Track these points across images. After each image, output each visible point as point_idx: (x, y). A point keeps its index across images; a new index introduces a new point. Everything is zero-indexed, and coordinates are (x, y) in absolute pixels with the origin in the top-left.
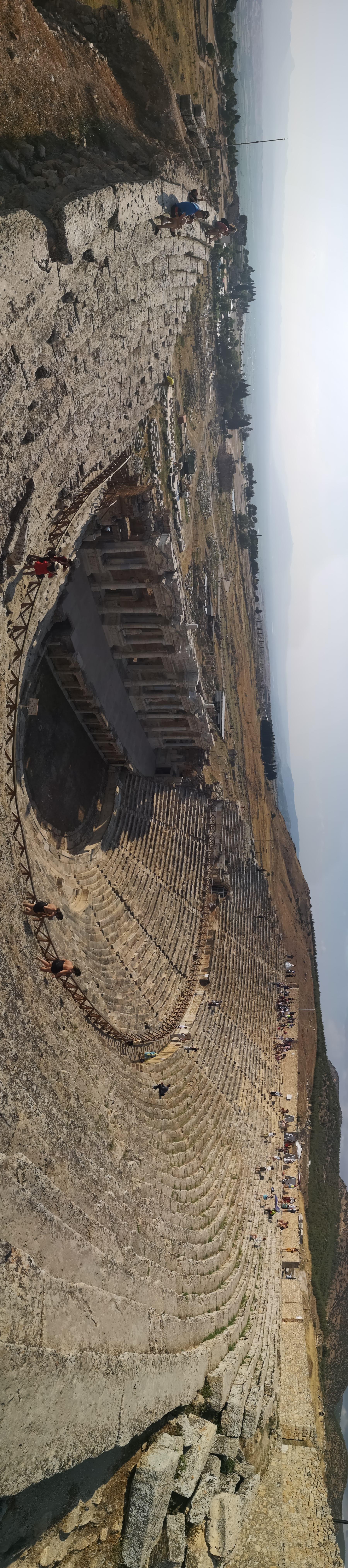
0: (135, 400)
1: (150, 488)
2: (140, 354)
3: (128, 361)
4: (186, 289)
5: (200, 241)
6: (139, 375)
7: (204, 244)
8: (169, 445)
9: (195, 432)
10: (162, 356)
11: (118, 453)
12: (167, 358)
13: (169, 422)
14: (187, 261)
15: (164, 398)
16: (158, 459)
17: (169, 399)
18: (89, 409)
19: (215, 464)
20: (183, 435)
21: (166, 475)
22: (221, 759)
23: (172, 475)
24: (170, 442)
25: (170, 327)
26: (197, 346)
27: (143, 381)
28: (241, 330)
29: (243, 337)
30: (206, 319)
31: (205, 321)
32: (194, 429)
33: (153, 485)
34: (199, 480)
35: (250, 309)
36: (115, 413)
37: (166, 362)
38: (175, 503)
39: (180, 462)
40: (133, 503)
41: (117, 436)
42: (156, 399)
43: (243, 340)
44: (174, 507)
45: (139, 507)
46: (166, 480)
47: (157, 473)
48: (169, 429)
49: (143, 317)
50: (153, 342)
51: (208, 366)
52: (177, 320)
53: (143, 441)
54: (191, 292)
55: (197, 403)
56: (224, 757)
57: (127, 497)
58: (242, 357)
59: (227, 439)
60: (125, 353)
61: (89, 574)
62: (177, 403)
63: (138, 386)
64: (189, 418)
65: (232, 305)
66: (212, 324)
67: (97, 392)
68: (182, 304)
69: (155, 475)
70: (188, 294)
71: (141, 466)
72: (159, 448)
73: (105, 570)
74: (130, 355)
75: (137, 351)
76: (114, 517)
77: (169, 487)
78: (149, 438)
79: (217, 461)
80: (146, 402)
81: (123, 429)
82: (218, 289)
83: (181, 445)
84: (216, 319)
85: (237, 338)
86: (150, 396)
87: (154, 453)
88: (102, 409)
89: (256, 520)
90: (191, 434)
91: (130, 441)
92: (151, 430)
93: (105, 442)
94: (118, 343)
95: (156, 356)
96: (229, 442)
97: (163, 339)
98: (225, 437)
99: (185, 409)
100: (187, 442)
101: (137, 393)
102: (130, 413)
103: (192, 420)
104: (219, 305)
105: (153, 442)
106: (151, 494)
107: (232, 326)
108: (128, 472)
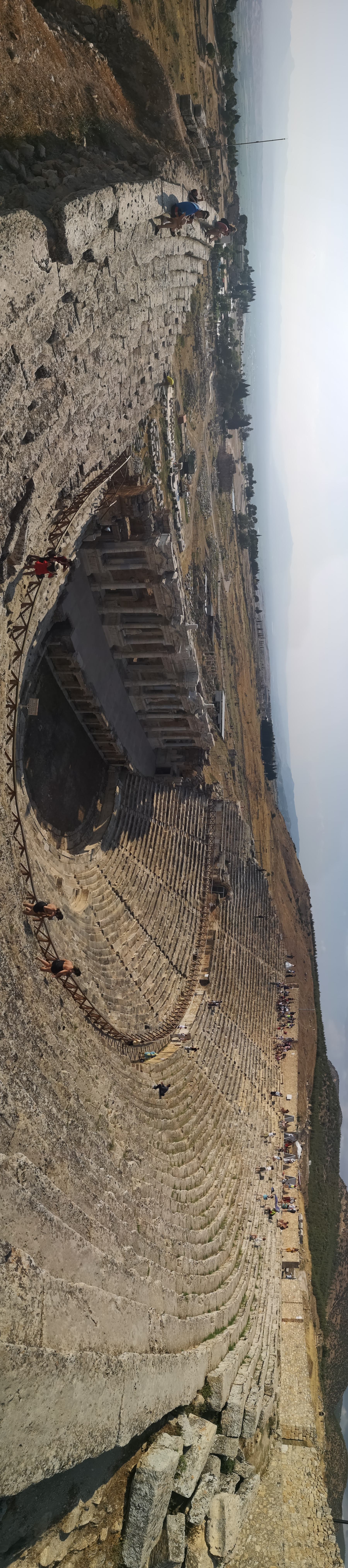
0: (135, 400)
1: (150, 488)
2: (140, 354)
3: (128, 361)
4: (186, 289)
5: (200, 241)
6: (139, 375)
7: (204, 244)
8: (169, 445)
9: (195, 432)
10: (162, 356)
11: (118, 453)
12: (167, 358)
13: (169, 422)
14: (187, 261)
15: (164, 398)
16: (158, 459)
17: (169, 399)
18: (89, 409)
19: (215, 464)
20: (183, 435)
21: (166, 475)
22: (221, 759)
23: (172, 475)
24: (170, 442)
25: (170, 327)
26: (197, 346)
27: (143, 381)
28: (241, 330)
29: (243, 337)
30: (206, 319)
31: (205, 321)
32: (194, 429)
33: (153, 485)
34: (199, 480)
35: (250, 309)
36: (115, 413)
37: (166, 362)
38: (175, 503)
39: (180, 462)
40: (133, 503)
41: (117, 436)
42: (156, 399)
43: (243, 340)
44: (174, 507)
45: (139, 507)
46: (166, 480)
47: (157, 473)
48: (169, 429)
49: (143, 317)
50: (153, 342)
51: (208, 366)
52: (177, 320)
53: (143, 441)
54: (191, 292)
55: (197, 403)
56: (224, 757)
57: (127, 497)
58: (242, 357)
59: (227, 439)
60: (125, 353)
61: (89, 574)
62: (177, 403)
63: (138, 386)
64: (189, 418)
65: (232, 305)
66: (212, 324)
67: (97, 392)
68: (182, 304)
69: (155, 475)
70: (188, 294)
71: (141, 466)
72: (159, 448)
73: (105, 570)
74: (130, 355)
75: (137, 351)
76: (114, 517)
77: (169, 487)
78: (149, 438)
79: (217, 461)
80: (146, 402)
81: (123, 429)
82: (218, 289)
83: (181, 445)
84: (216, 319)
85: (237, 338)
86: (150, 396)
87: (154, 453)
88: (102, 409)
89: (256, 520)
90: (191, 434)
91: (130, 441)
92: (151, 430)
93: (105, 442)
94: (118, 343)
95: (156, 356)
96: (229, 442)
97: (163, 339)
98: (225, 437)
99: (185, 409)
100: (187, 442)
101: (137, 393)
102: (130, 413)
103: (192, 420)
104: (219, 305)
105: (153, 442)
106: (151, 494)
107: (232, 326)
108: (128, 472)
